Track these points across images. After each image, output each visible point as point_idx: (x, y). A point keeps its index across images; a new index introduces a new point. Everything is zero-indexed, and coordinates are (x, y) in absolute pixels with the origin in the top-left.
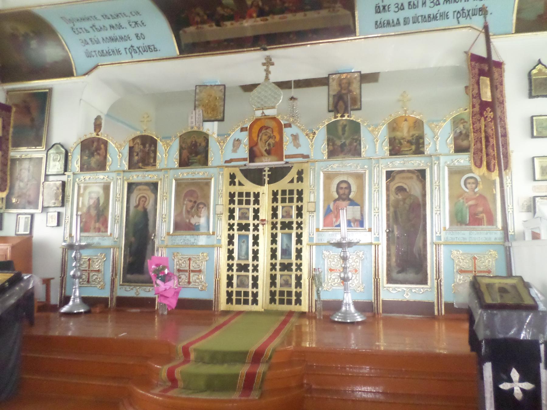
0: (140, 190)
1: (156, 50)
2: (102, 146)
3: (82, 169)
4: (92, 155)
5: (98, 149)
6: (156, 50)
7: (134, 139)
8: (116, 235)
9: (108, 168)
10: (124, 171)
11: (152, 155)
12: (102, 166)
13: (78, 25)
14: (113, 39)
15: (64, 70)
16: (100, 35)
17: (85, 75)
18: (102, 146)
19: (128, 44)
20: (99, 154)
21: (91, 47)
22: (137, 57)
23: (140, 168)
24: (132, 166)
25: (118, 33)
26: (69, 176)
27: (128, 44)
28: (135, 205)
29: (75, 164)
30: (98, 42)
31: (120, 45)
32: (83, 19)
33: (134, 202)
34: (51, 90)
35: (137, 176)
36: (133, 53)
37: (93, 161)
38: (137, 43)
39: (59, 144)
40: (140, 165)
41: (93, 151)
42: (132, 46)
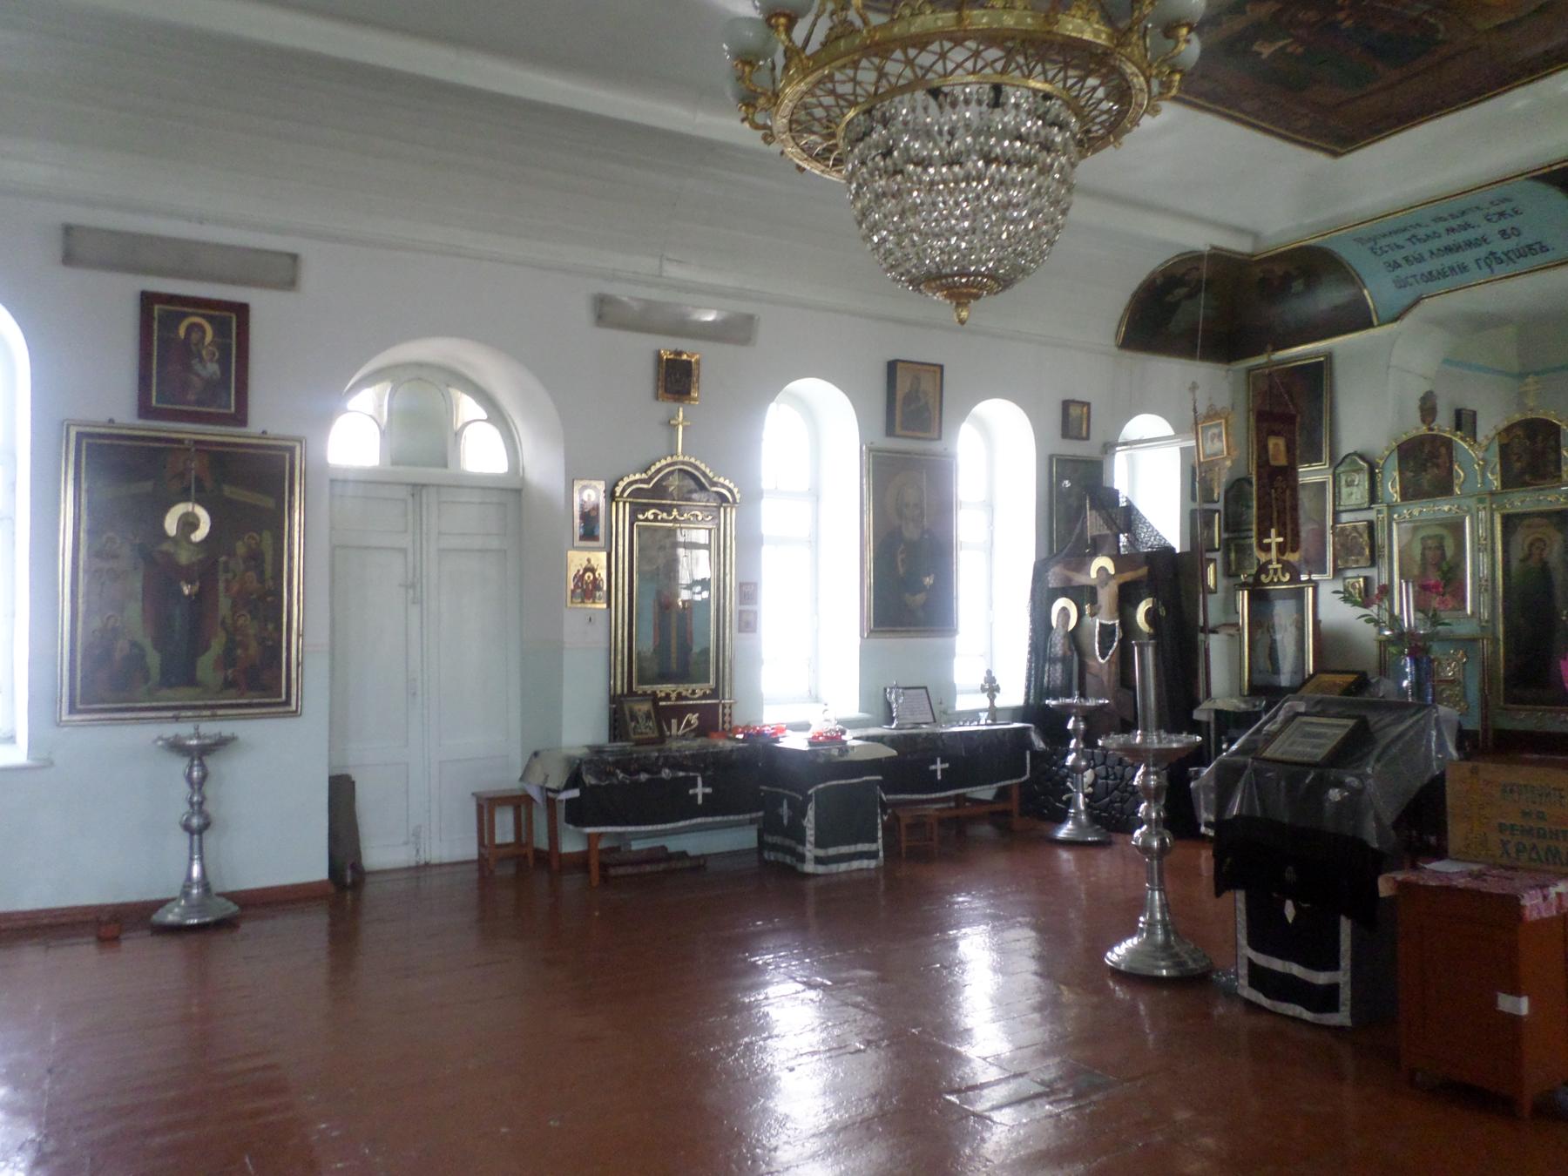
0: (1529, 526)
1: (1544, 249)
2: (1443, 450)
3: (1405, 496)
4: (1422, 467)
5: (1434, 455)
6: (1544, 249)
7: (1508, 430)
8: (1485, 614)
9: (1457, 490)
10: (1492, 493)
11: (1552, 457)
12: (1444, 488)
13: (1383, 242)
14: (1449, 250)
15: (1357, 318)
16: (1423, 248)
17: (1395, 319)
18: (1443, 450)
19: (1482, 251)
20: (1438, 466)
21: (1406, 271)
22: (1501, 270)
23: (1529, 484)
24: (1510, 481)
25: (1461, 237)
26: (1379, 512)
27: (1482, 251)
28: (1521, 555)
29: (1391, 488)
30: (1420, 259)
31: (1467, 257)
32: (1396, 232)
33: (1518, 553)
34: (1329, 356)
35: (1521, 501)
36: (1494, 265)
37: (1426, 479)
38: (1500, 246)
39: (1355, 453)
40: (1527, 478)
41: (1426, 464)
42: (1492, 253)
